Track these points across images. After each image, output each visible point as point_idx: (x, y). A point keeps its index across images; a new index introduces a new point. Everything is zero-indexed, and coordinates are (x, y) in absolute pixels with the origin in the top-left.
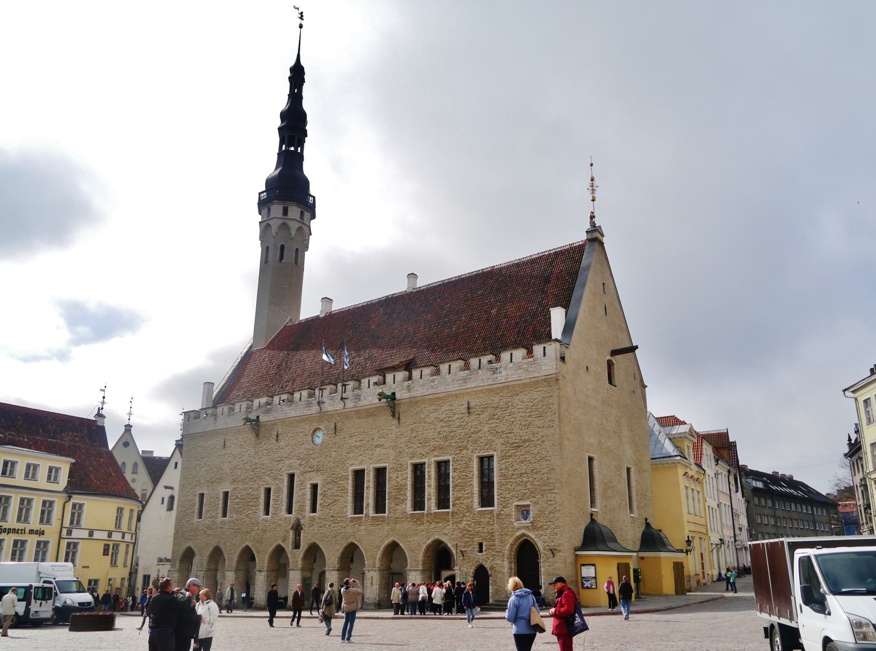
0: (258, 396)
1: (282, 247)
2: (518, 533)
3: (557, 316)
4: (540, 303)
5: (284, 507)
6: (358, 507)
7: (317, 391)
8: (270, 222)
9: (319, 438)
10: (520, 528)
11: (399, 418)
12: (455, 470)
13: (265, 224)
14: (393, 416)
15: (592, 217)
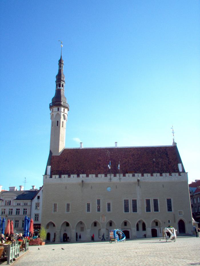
0: (83, 173)
1: (63, 122)
2: (180, 218)
3: (180, 165)
4: (169, 160)
5: (97, 209)
6: (127, 210)
7: (108, 175)
8: (59, 112)
9: (109, 189)
10: (181, 217)
11: (140, 187)
12: (160, 202)
13: (57, 113)
14: (139, 186)
15: (174, 140)
